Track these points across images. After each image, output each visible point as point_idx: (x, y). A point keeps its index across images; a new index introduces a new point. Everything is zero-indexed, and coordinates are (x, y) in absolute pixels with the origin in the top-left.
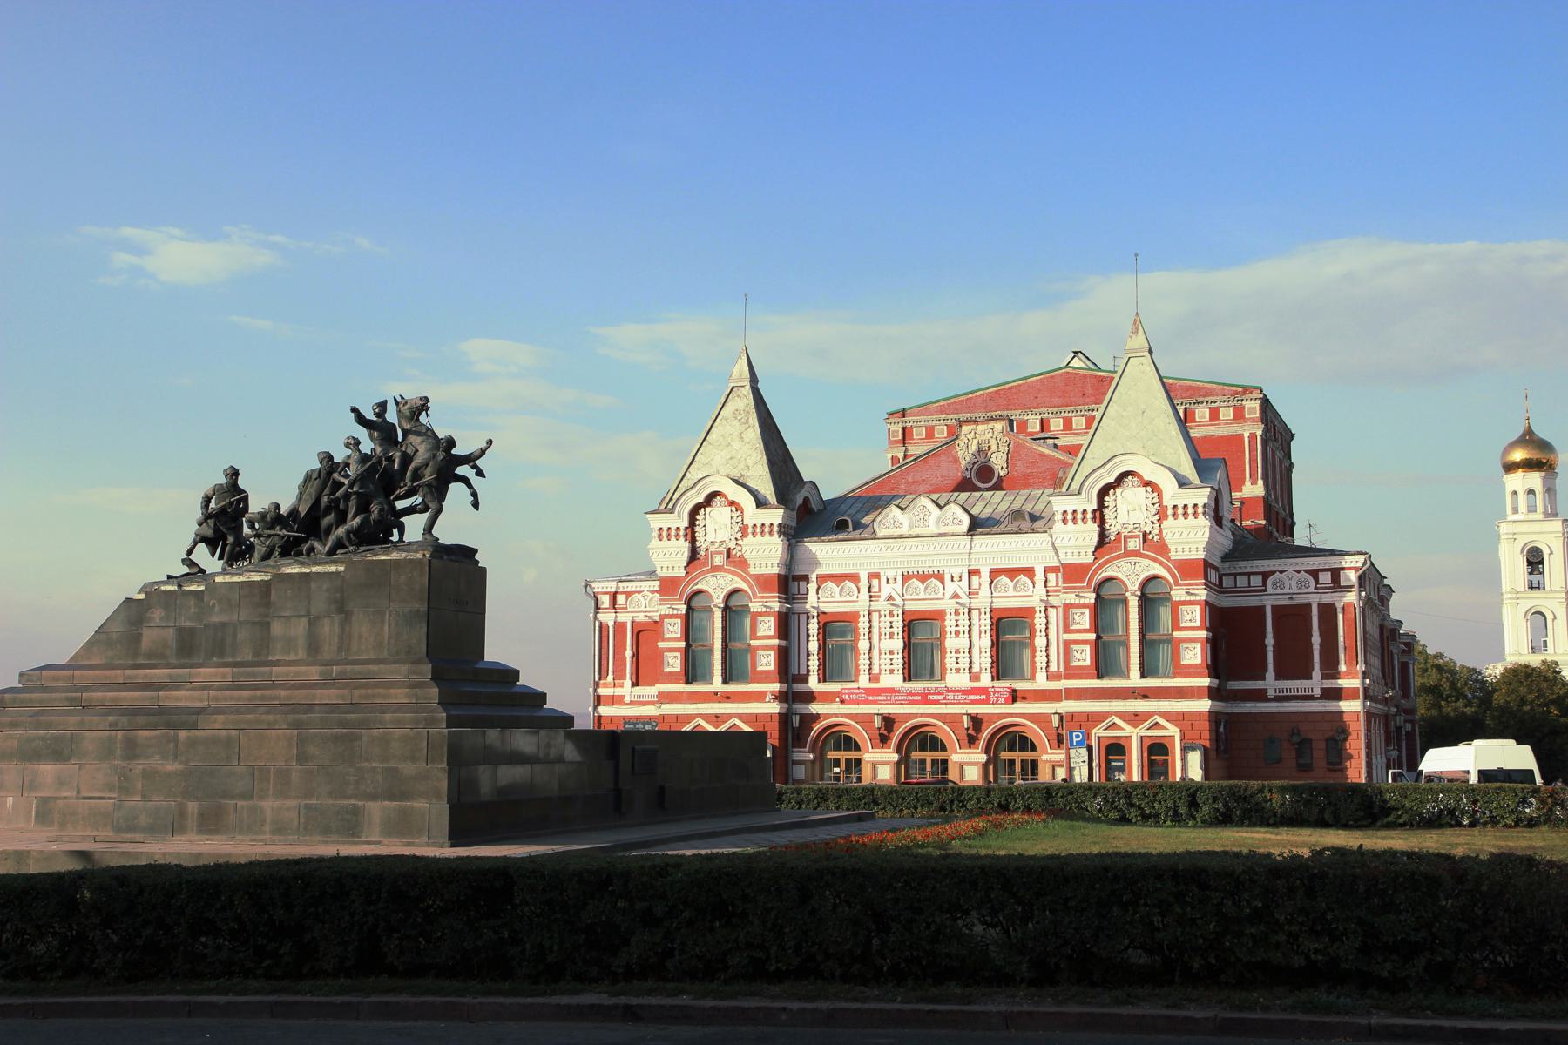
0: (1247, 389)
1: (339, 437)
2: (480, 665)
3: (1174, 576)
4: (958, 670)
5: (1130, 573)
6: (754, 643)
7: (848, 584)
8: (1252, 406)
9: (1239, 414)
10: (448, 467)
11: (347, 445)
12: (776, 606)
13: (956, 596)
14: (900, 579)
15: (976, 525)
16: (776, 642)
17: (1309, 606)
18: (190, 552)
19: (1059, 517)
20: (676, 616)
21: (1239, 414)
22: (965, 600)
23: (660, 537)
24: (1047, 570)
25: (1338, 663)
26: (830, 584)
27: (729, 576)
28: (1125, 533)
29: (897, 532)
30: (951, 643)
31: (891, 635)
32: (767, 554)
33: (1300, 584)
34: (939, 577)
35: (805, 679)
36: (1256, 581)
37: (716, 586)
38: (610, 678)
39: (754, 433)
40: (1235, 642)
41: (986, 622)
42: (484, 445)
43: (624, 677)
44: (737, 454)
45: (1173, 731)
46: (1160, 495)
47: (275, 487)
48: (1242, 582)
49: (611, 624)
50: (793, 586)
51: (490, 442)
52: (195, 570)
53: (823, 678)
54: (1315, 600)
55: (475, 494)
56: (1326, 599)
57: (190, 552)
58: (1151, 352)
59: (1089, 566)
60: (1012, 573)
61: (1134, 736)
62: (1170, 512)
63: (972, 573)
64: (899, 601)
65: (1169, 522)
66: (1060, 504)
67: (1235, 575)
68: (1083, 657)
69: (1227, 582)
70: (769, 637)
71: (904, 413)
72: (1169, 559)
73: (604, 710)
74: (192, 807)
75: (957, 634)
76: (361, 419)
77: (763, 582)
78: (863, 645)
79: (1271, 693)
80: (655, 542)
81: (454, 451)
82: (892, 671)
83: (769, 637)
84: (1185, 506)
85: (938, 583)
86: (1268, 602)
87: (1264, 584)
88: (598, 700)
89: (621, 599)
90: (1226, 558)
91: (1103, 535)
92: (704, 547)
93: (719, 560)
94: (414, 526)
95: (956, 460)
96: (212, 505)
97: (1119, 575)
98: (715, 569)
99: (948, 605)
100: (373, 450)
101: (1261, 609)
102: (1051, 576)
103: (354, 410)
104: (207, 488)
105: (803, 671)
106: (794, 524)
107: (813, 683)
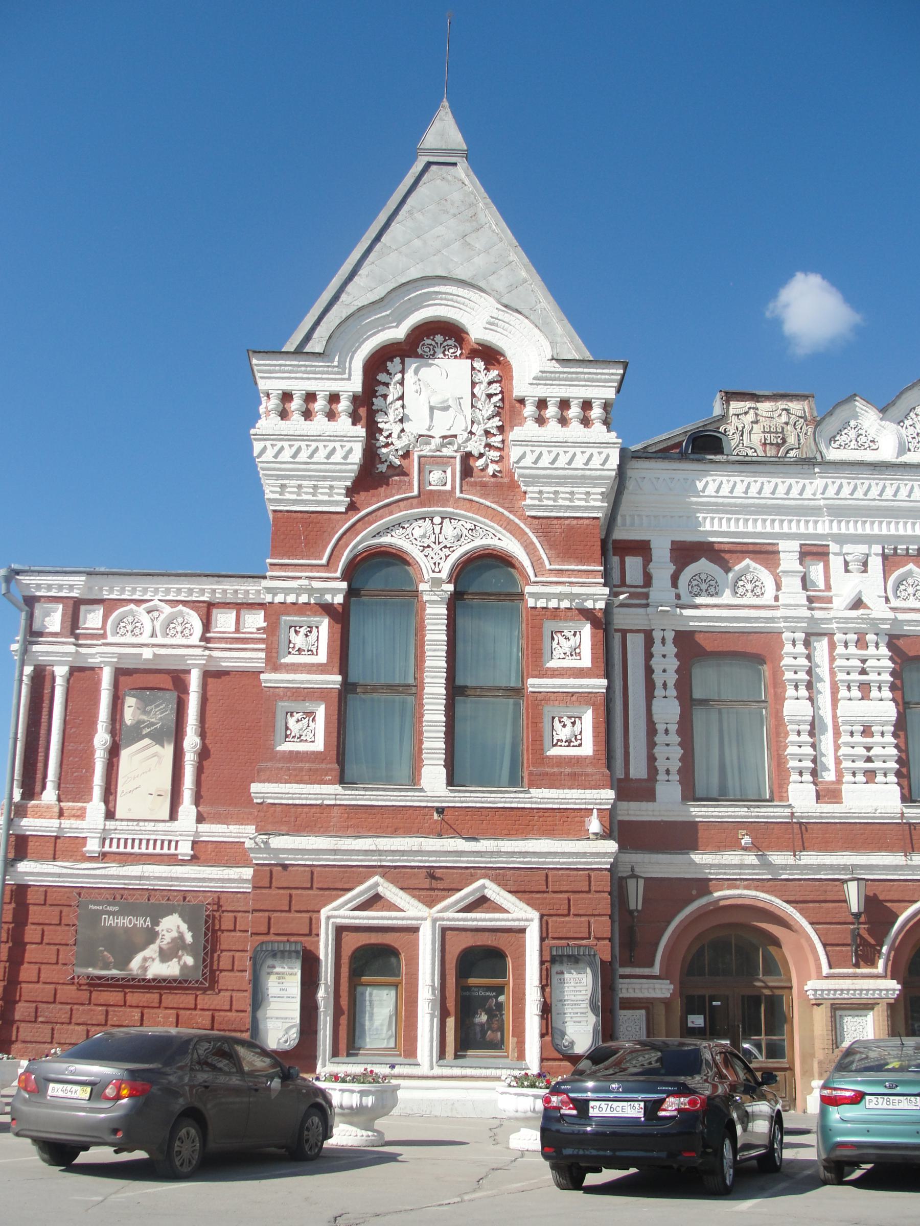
12: (596, 595)
14: (876, 563)
29: (869, 456)
31: (865, 688)
38: (49, 795)
43: (83, 794)
49: (60, 672)
73: (30, 870)
77: (563, 538)
82: (870, 776)
88: (21, 847)
89: (92, 619)
92: (399, 444)
98: (426, 497)
105: (638, 770)
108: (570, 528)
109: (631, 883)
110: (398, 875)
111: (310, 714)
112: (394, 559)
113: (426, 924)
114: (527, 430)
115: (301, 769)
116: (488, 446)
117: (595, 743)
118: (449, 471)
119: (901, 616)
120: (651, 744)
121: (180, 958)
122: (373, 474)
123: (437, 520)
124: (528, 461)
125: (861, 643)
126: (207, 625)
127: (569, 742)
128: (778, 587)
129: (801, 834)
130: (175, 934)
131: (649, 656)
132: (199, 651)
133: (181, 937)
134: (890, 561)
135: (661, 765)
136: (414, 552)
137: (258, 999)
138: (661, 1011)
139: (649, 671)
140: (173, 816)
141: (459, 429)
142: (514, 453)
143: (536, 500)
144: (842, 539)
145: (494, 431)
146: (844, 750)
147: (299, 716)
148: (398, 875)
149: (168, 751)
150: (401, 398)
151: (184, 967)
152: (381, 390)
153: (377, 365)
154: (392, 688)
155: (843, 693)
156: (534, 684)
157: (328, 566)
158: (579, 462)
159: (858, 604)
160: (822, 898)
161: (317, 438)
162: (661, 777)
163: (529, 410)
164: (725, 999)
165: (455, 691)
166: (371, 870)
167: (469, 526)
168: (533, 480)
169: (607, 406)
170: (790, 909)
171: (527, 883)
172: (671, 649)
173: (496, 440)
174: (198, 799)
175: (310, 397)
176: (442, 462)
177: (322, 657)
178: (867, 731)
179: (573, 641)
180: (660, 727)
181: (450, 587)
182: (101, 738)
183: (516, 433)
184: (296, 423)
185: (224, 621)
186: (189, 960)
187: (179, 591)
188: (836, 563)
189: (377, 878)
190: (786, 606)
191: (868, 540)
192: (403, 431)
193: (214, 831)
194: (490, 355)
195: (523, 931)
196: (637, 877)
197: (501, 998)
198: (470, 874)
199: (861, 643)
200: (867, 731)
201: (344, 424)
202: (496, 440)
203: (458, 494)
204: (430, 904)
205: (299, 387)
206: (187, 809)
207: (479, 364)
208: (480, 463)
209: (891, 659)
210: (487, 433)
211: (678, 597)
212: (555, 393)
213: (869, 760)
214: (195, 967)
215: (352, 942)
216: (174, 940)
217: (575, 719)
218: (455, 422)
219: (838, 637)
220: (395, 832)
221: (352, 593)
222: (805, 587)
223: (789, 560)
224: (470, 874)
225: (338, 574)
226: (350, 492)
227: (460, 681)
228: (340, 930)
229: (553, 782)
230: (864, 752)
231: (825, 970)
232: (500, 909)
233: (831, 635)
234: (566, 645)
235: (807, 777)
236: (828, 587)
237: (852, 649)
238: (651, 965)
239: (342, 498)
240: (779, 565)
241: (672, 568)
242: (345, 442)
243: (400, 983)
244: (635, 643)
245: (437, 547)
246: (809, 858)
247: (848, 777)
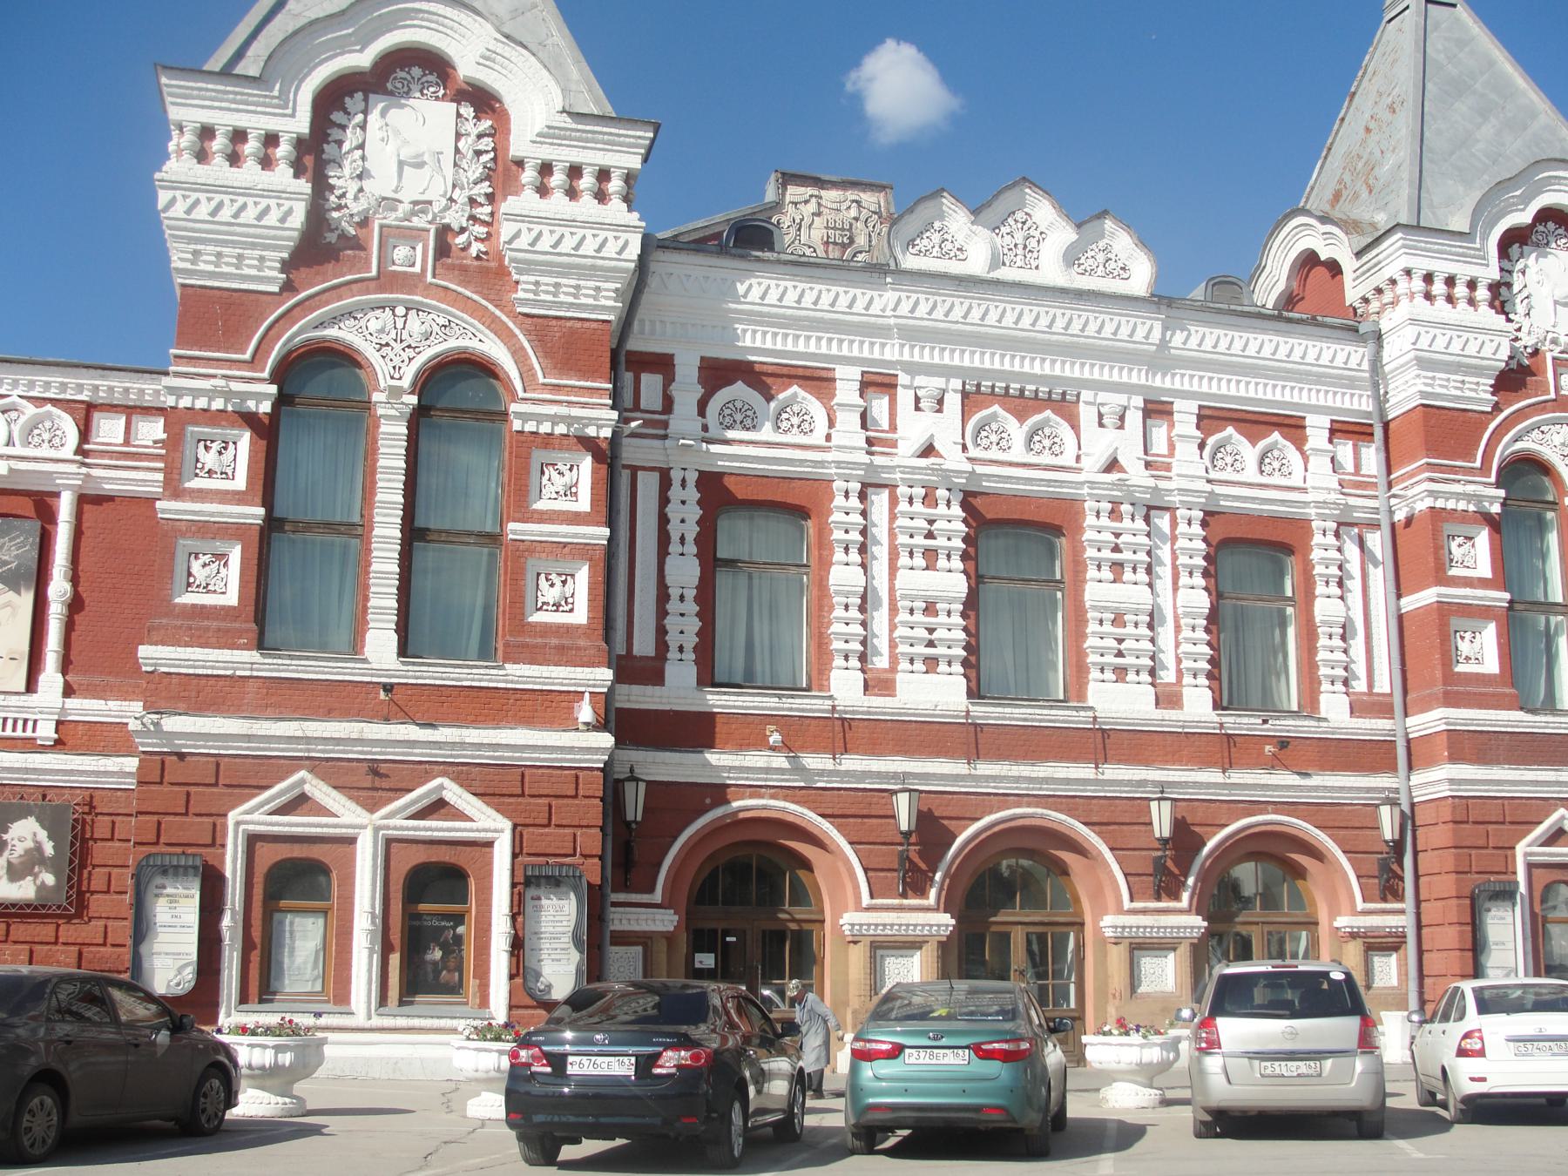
12: (601, 420)
14: (953, 402)
22: (1136, 474)
24: (1339, 430)
29: (954, 268)
31: (931, 555)
34: (1066, 407)
41: (1192, 543)
60: (1255, 423)
63: (1156, 410)
64: (953, 459)
70: (575, 518)
75: (1117, 567)
77: (562, 344)
82: (931, 663)
83: (575, 518)
92: (355, 208)
93: (410, 257)
98: (388, 280)
102: (1345, 450)
105: (644, 645)
108: (572, 331)
109: (629, 788)
110: (332, 770)
111: (221, 557)
112: (342, 358)
113: (365, 832)
114: (525, 201)
115: (207, 629)
116: (472, 218)
117: (591, 608)
118: (419, 248)
119: (980, 469)
120: (662, 613)
121: (36, 876)
122: (319, 247)
123: (400, 311)
124: (523, 242)
125: (929, 499)
126: (85, 435)
127: (557, 605)
128: (831, 424)
129: (843, 733)
130: (30, 844)
131: (664, 501)
132: (73, 468)
133: (38, 848)
134: (971, 400)
135: (673, 639)
136: (368, 351)
137: (141, 928)
138: (662, 946)
139: (663, 520)
140: (31, 686)
141: (436, 192)
142: (506, 230)
143: (529, 293)
144: (913, 369)
145: (481, 200)
146: (901, 631)
147: (207, 558)
148: (332, 770)
149: (27, 599)
150: (361, 146)
151: (42, 888)
152: (335, 133)
153: (334, 99)
154: (330, 527)
155: (904, 560)
156: (516, 530)
157: (253, 363)
158: (589, 248)
159: (928, 450)
160: (865, 812)
161: (246, 191)
162: (673, 654)
163: (529, 175)
164: (742, 935)
165: (413, 534)
166: (295, 763)
167: (442, 321)
168: (528, 267)
169: (629, 178)
170: (825, 825)
171: (499, 784)
172: (693, 494)
173: (484, 212)
174: (65, 666)
175: (239, 136)
177: (240, 483)
178: (930, 609)
179: (569, 478)
180: (674, 593)
181: (413, 400)
183: (510, 205)
184: (219, 171)
185: (109, 430)
186: (49, 879)
187: (47, 385)
188: (905, 398)
189: (303, 774)
190: (840, 448)
191: (947, 372)
192: (361, 190)
193: (86, 708)
194: (482, 100)
195: (489, 844)
196: (637, 780)
197: (461, 930)
198: (424, 771)
199: (929, 499)
200: (930, 609)
201: (282, 175)
203: (429, 278)
204: (372, 807)
205: (225, 120)
206: (51, 677)
207: (468, 111)
208: (461, 240)
209: (964, 521)
210: (472, 202)
211: (705, 428)
213: (931, 644)
214: (58, 886)
215: (268, 856)
216: (28, 852)
217: (566, 578)
218: (431, 184)
219: (902, 490)
220: (328, 714)
221: (283, 400)
222: (864, 426)
223: (847, 390)
224: (424, 771)
225: (266, 374)
226: (286, 266)
227: (420, 522)
228: (253, 840)
229: (534, 655)
230: (925, 634)
231: (866, 900)
232: (461, 816)
233: (892, 487)
234: (560, 482)
235: (854, 662)
236: (893, 427)
237: (918, 507)
238: (651, 890)
239: (275, 274)
240: (834, 395)
241: (699, 391)
242: (282, 199)
243: (331, 908)
244: (648, 485)
245: (398, 347)
246: (852, 763)
247: (904, 665)
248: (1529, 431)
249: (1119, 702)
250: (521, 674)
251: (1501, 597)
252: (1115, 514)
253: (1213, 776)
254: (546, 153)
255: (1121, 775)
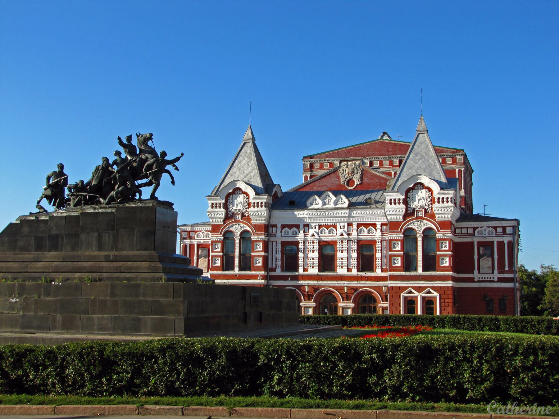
0: (458, 151)
1: (110, 150)
2: (174, 256)
3: (437, 228)
4: (342, 267)
5: (419, 226)
6: (253, 254)
7: (294, 229)
8: (460, 158)
9: (454, 161)
10: (159, 166)
11: (116, 155)
13: (342, 235)
14: (317, 227)
15: (352, 206)
16: (263, 253)
17: (493, 242)
18: (39, 202)
19: (388, 202)
20: (219, 242)
21: (454, 161)
22: (346, 236)
23: (212, 207)
24: (382, 225)
25: (505, 267)
26: (286, 229)
27: (242, 225)
28: (417, 209)
29: (317, 207)
30: (339, 255)
32: (259, 215)
33: (489, 233)
34: (335, 226)
35: (274, 270)
36: (470, 231)
37: (237, 229)
39: (254, 162)
40: (463, 257)
42: (180, 155)
44: (245, 173)
45: (436, 294)
46: (432, 194)
47: (81, 173)
48: (464, 231)
50: (270, 229)
51: (182, 154)
52: (42, 210)
53: (282, 270)
54: (496, 240)
55: (172, 178)
56: (500, 239)
57: (39, 202)
58: (427, 131)
59: (401, 223)
60: (366, 225)
61: (419, 296)
62: (436, 200)
63: (350, 225)
65: (436, 205)
66: (388, 197)
67: (461, 228)
68: (399, 262)
69: (458, 231)
71: (311, 157)
72: (435, 221)
74: (59, 317)
75: (342, 251)
76: (121, 143)
77: (257, 228)
78: (301, 255)
79: (476, 279)
80: (210, 209)
81: (166, 158)
82: (313, 267)
84: (443, 198)
85: (334, 229)
86: (476, 240)
87: (474, 232)
89: (193, 234)
90: (457, 221)
91: (407, 210)
93: (238, 217)
94: (146, 192)
95: (338, 177)
96: (51, 181)
97: (414, 227)
99: (337, 238)
100: (126, 157)
101: (473, 243)
103: (119, 138)
104: (49, 173)
105: (274, 266)
106: (271, 202)
107: (278, 272)
112: (231, 232)
114: (252, 209)
125: (313, 242)
134: (320, 227)
168: (253, 217)
169: (265, 203)
172: (280, 244)
176: (239, 214)
177: (220, 250)
178: (313, 259)
182: (195, 257)
184: (214, 209)
202: (248, 210)
212: (256, 201)
218: (240, 207)
220: (231, 279)
229: (255, 270)
244: (274, 243)
248: (411, 224)
249: (342, 271)
250: (253, 273)
251: (402, 253)
252: (342, 242)
253: (356, 282)
254: (254, 201)
255: (341, 283)
